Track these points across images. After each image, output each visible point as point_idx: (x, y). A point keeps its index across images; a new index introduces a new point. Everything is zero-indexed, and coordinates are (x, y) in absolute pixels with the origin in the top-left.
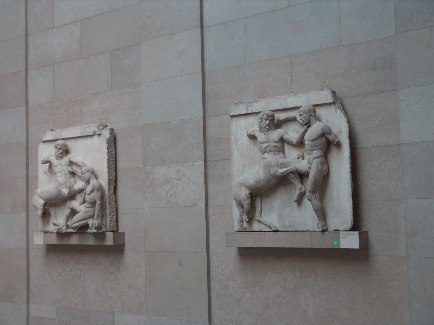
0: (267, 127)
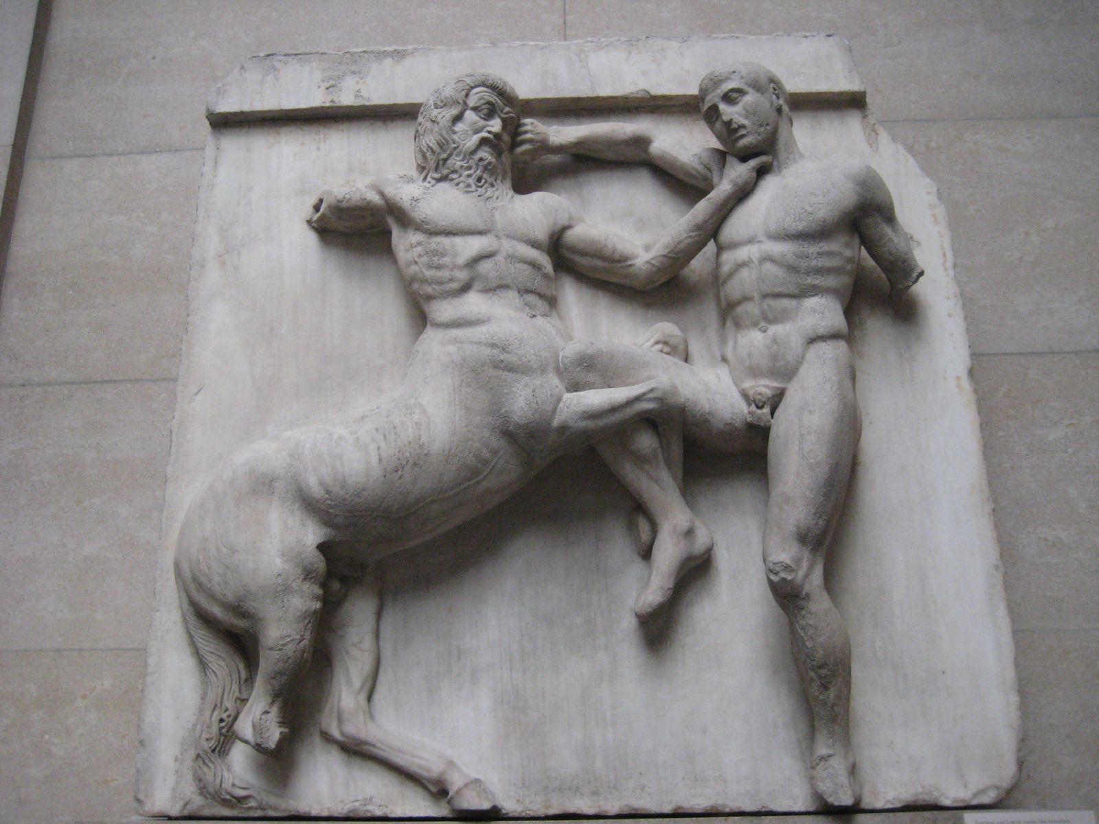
0: (486, 154)
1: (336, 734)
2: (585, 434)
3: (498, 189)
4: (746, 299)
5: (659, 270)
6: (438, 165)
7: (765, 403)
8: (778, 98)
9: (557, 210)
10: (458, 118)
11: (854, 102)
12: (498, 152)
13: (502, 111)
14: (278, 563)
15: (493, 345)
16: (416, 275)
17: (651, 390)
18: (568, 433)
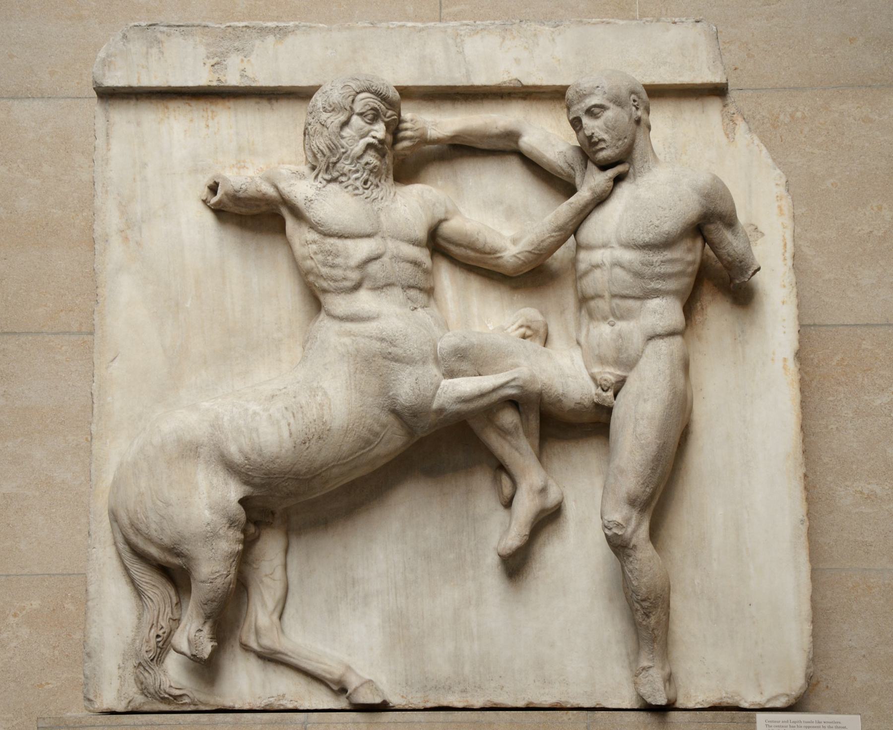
0: (371, 158)
2: (458, 414)
4: (600, 296)
5: (524, 263)
9: (434, 204)
12: (382, 155)
13: (385, 116)
14: (207, 515)
15: (382, 340)
17: (514, 380)
18: (445, 413)
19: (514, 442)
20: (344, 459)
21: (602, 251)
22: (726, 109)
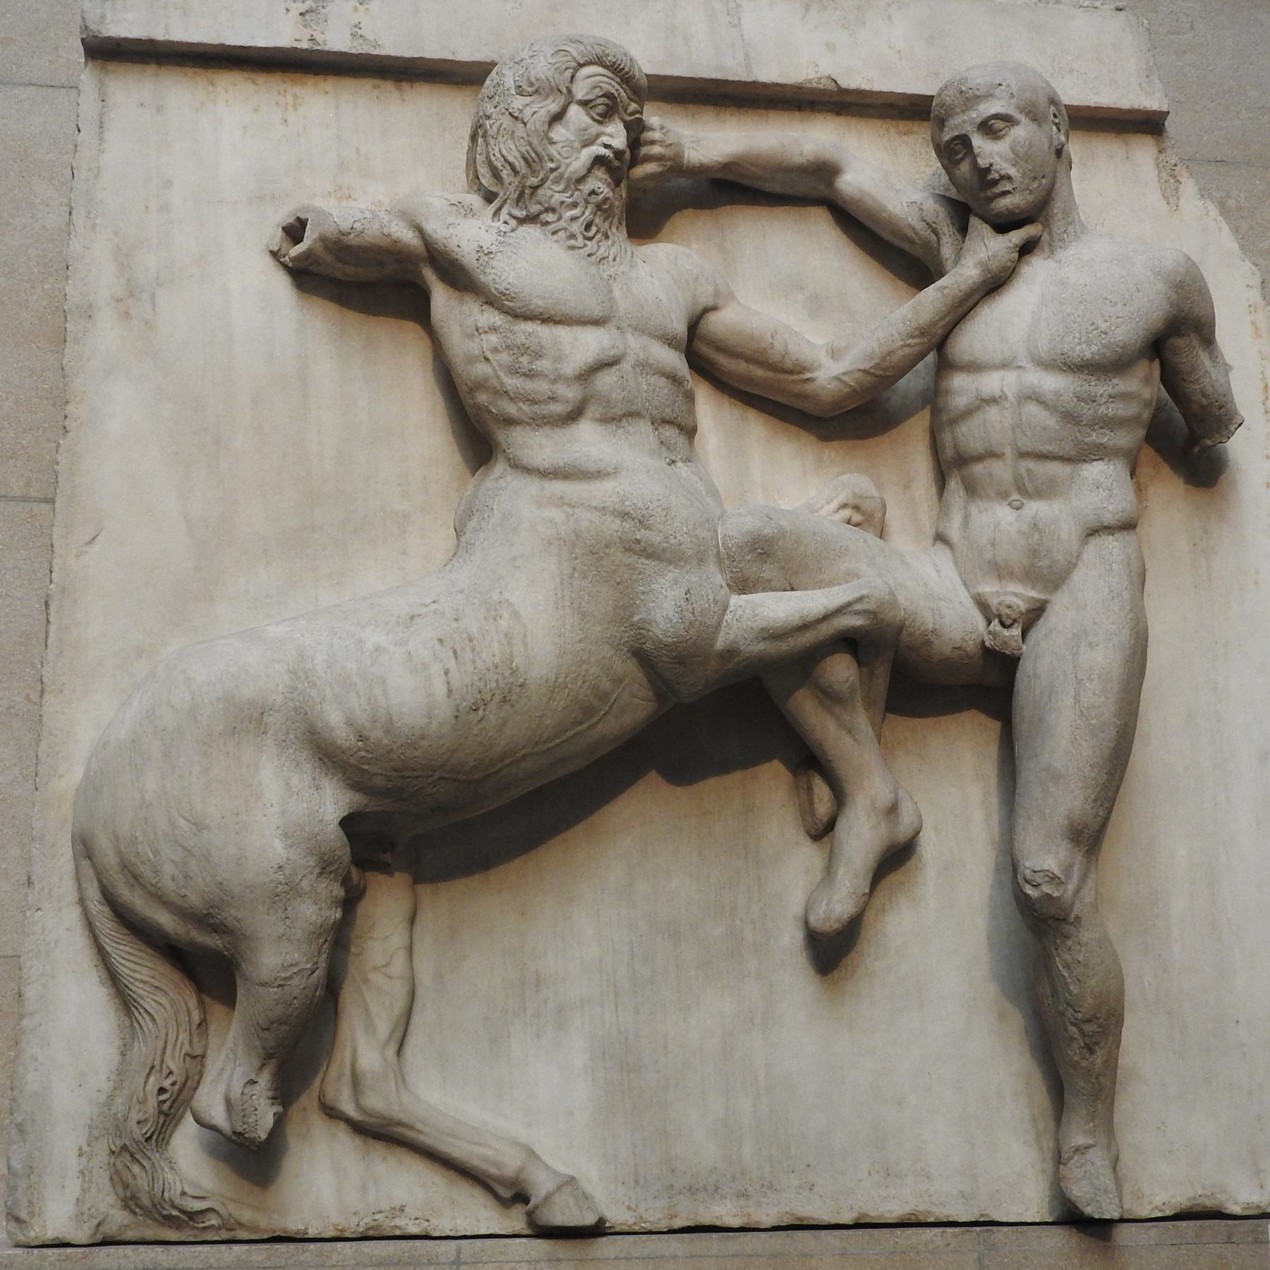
0: (599, 183)
1: (349, 1109)
3: (613, 244)
6: (522, 194)
7: (1015, 621)
8: (1059, 130)
9: (696, 279)
10: (557, 117)
11: (1147, 125)
13: (626, 111)
14: (278, 849)
15: (624, 515)
16: (487, 380)
17: (861, 599)
19: (846, 717)
20: (545, 742)
21: (1002, 373)
22: (1162, 157)
